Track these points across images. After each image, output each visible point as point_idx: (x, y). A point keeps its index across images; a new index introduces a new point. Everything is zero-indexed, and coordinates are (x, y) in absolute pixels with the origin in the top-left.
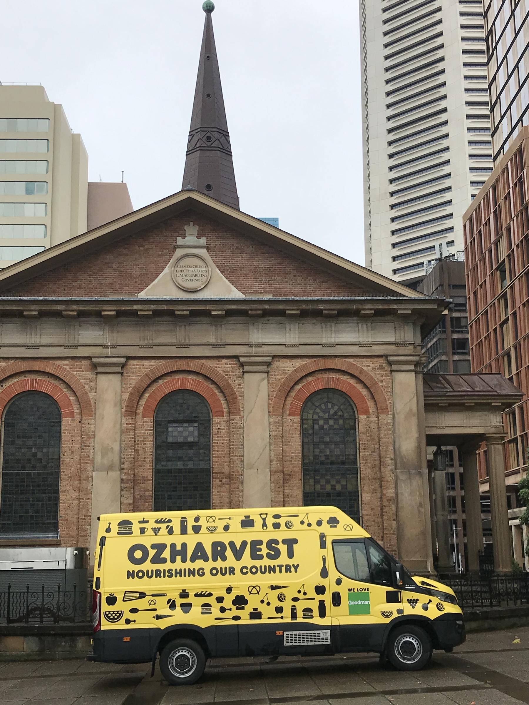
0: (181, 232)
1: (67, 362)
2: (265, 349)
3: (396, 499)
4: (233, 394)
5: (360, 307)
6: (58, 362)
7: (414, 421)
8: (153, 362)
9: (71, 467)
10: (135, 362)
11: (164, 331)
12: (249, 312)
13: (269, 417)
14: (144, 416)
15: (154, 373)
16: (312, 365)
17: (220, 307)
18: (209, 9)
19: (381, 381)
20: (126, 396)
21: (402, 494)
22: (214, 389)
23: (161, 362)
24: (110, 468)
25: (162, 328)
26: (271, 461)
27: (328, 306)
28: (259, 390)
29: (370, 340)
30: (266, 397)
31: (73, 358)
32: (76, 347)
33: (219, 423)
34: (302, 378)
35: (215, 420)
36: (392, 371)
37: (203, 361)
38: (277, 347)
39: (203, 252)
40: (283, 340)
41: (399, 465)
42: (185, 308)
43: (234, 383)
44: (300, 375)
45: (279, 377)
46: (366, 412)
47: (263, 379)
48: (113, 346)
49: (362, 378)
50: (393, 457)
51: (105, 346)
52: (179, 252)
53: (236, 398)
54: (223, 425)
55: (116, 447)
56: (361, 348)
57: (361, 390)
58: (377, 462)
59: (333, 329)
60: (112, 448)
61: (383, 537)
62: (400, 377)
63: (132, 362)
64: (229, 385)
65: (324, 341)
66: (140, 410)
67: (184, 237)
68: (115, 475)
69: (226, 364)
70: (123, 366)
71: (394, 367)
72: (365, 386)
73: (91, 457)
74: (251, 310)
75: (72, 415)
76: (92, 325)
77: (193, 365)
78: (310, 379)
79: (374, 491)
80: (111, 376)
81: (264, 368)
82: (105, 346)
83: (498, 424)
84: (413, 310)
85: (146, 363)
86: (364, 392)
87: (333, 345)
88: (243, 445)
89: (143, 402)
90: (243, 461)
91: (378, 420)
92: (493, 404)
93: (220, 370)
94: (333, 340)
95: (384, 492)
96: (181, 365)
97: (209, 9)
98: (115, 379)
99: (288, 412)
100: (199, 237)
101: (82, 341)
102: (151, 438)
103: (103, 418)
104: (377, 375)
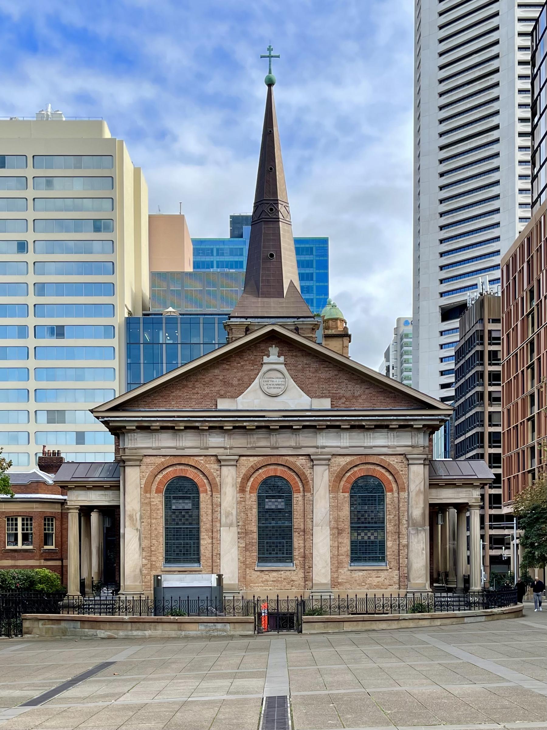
3: (407, 546)
4: (306, 478)
6: (196, 458)
8: (256, 458)
9: (207, 524)
13: (330, 494)
14: (250, 493)
15: (256, 465)
19: (402, 471)
22: (294, 475)
24: (230, 525)
26: (330, 522)
28: (323, 476)
29: (395, 444)
31: (205, 456)
32: (207, 448)
33: (297, 498)
36: (408, 464)
37: (288, 458)
40: (338, 444)
41: (411, 524)
43: (308, 472)
44: (349, 467)
45: (336, 468)
47: (326, 470)
48: (231, 448)
51: (225, 448)
53: (308, 481)
56: (389, 449)
57: (388, 476)
58: (397, 522)
59: (371, 436)
61: (399, 568)
62: (412, 468)
64: (304, 473)
65: (365, 445)
66: (248, 489)
68: (234, 530)
69: (302, 459)
77: (281, 460)
78: (356, 469)
80: (230, 467)
82: (225, 448)
85: (251, 459)
86: (390, 478)
87: (371, 447)
89: (250, 484)
93: (298, 463)
95: (401, 541)
96: (273, 460)
98: (232, 470)
99: (341, 491)
101: (211, 445)
102: (255, 506)
103: (225, 494)
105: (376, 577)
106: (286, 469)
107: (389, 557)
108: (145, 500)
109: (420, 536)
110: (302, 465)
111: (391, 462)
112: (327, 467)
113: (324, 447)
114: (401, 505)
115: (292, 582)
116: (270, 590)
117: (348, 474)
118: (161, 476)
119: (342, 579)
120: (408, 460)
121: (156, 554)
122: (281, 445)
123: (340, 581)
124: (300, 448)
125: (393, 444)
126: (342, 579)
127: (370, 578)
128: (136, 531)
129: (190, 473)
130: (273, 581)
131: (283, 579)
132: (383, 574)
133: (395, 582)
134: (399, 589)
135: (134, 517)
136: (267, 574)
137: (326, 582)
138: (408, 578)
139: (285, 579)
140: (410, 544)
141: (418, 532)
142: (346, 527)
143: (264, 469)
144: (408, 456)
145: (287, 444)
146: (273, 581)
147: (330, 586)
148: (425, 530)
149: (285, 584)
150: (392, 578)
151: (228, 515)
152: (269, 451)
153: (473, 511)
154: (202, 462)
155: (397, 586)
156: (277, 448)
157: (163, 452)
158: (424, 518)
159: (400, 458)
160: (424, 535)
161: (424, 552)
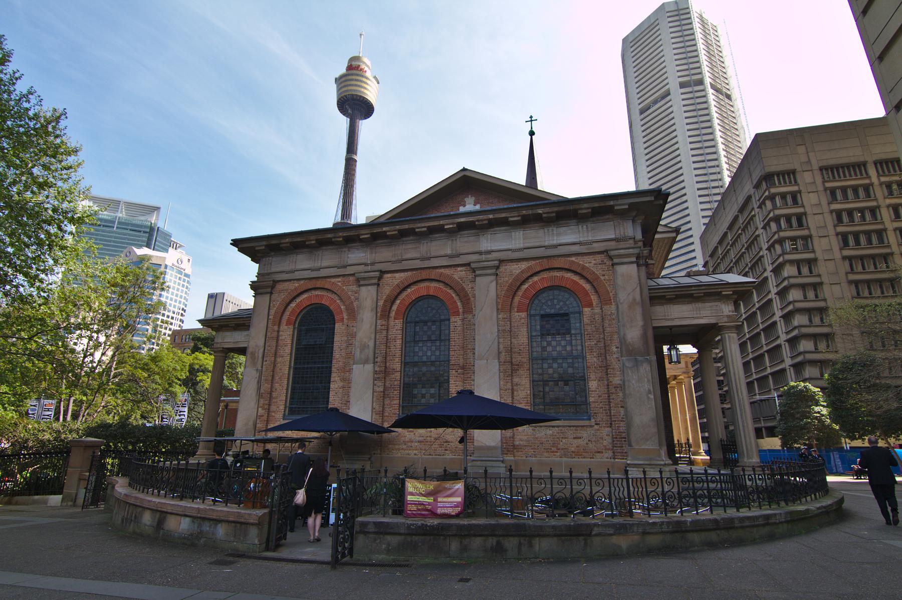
0: (463, 203)
1: (339, 279)
2: (494, 256)
3: (622, 387)
4: (466, 295)
5: (577, 207)
6: (333, 280)
8: (402, 274)
9: (339, 361)
10: (389, 275)
11: (412, 248)
12: (477, 223)
13: (498, 314)
14: (395, 319)
15: (403, 283)
16: (535, 265)
17: (450, 221)
18: (532, 133)
19: (603, 275)
20: (381, 303)
21: (629, 381)
22: (452, 293)
23: (409, 273)
24: (366, 362)
25: (410, 246)
26: (499, 353)
27: (547, 210)
28: (488, 291)
29: (590, 238)
30: (495, 297)
31: (343, 276)
32: (345, 267)
33: (456, 322)
34: (528, 278)
36: (613, 265)
37: (442, 270)
38: (504, 252)
40: (510, 247)
41: (624, 352)
42: (423, 225)
43: (468, 287)
44: (525, 276)
45: (507, 279)
46: (590, 305)
47: (492, 282)
48: (373, 264)
49: (584, 274)
50: (618, 345)
51: (366, 264)
53: (469, 299)
54: (459, 323)
55: (371, 344)
56: (582, 247)
57: (584, 285)
58: (603, 351)
59: (555, 232)
60: (368, 345)
61: (611, 424)
62: (621, 269)
63: (386, 276)
64: (463, 289)
65: (546, 244)
66: (393, 314)
67: (464, 206)
68: (369, 367)
69: (461, 271)
70: (380, 278)
71: (616, 261)
72: (588, 281)
73: (353, 353)
74: (478, 221)
75: (342, 320)
76: (358, 249)
77: (433, 274)
78: (536, 279)
79: (600, 379)
80: (369, 287)
81: (493, 271)
82: (366, 264)
83: (731, 313)
84: (630, 205)
85: (397, 275)
86: (587, 287)
87: (555, 246)
88: (474, 339)
89: (395, 307)
90: (474, 354)
91: (602, 312)
92: (723, 293)
93: (456, 277)
94: (555, 242)
95: (611, 379)
96: (424, 275)
97: (532, 133)
98: (373, 289)
99: (516, 310)
100: (475, 205)
101: (350, 262)
102: (400, 337)
103: (362, 321)
104: (598, 272)
105: (575, 438)
106: (441, 286)
107: (593, 405)
108: (272, 333)
109: (642, 370)
110: (461, 279)
111: (587, 265)
112: (493, 277)
113: (489, 252)
114: (606, 325)
115: (445, 444)
116: (415, 454)
117: (525, 286)
118: (294, 305)
119: (521, 440)
120: (611, 258)
121: (276, 402)
122: (433, 254)
123: (517, 443)
124: (459, 255)
125: (586, 239)
126: (521, 440)
127: (564, 441)
128: (255, 372)
129: (326, 299)
130: (419, 442)
131: (433, 439)
132: (585, 434)
133: (605, 446)
134: (615, 459)
135: (256, 355)
136: (411, 431)
137: (493, 444)
138: (627, 440)
139: (436, 439)
140: (626, 383)
141: (637, 364)
142: (524, 360)
143: (413, 288)
144: (612, 253)
145: (442, 253)
146: (419, 442)
147: (499, 451)
148: (650, 362)
149: (437, 446)
150: (601, 441)
151: (364, 347)
152: (418, 264)
153: (727, 335)
154: (339, 284)
155: (610, 454)
156: (429, 259)
157: (297, 275)
158: (646, 343)
159: (599, 258)
160: (648, 368)
161: (652, 397)
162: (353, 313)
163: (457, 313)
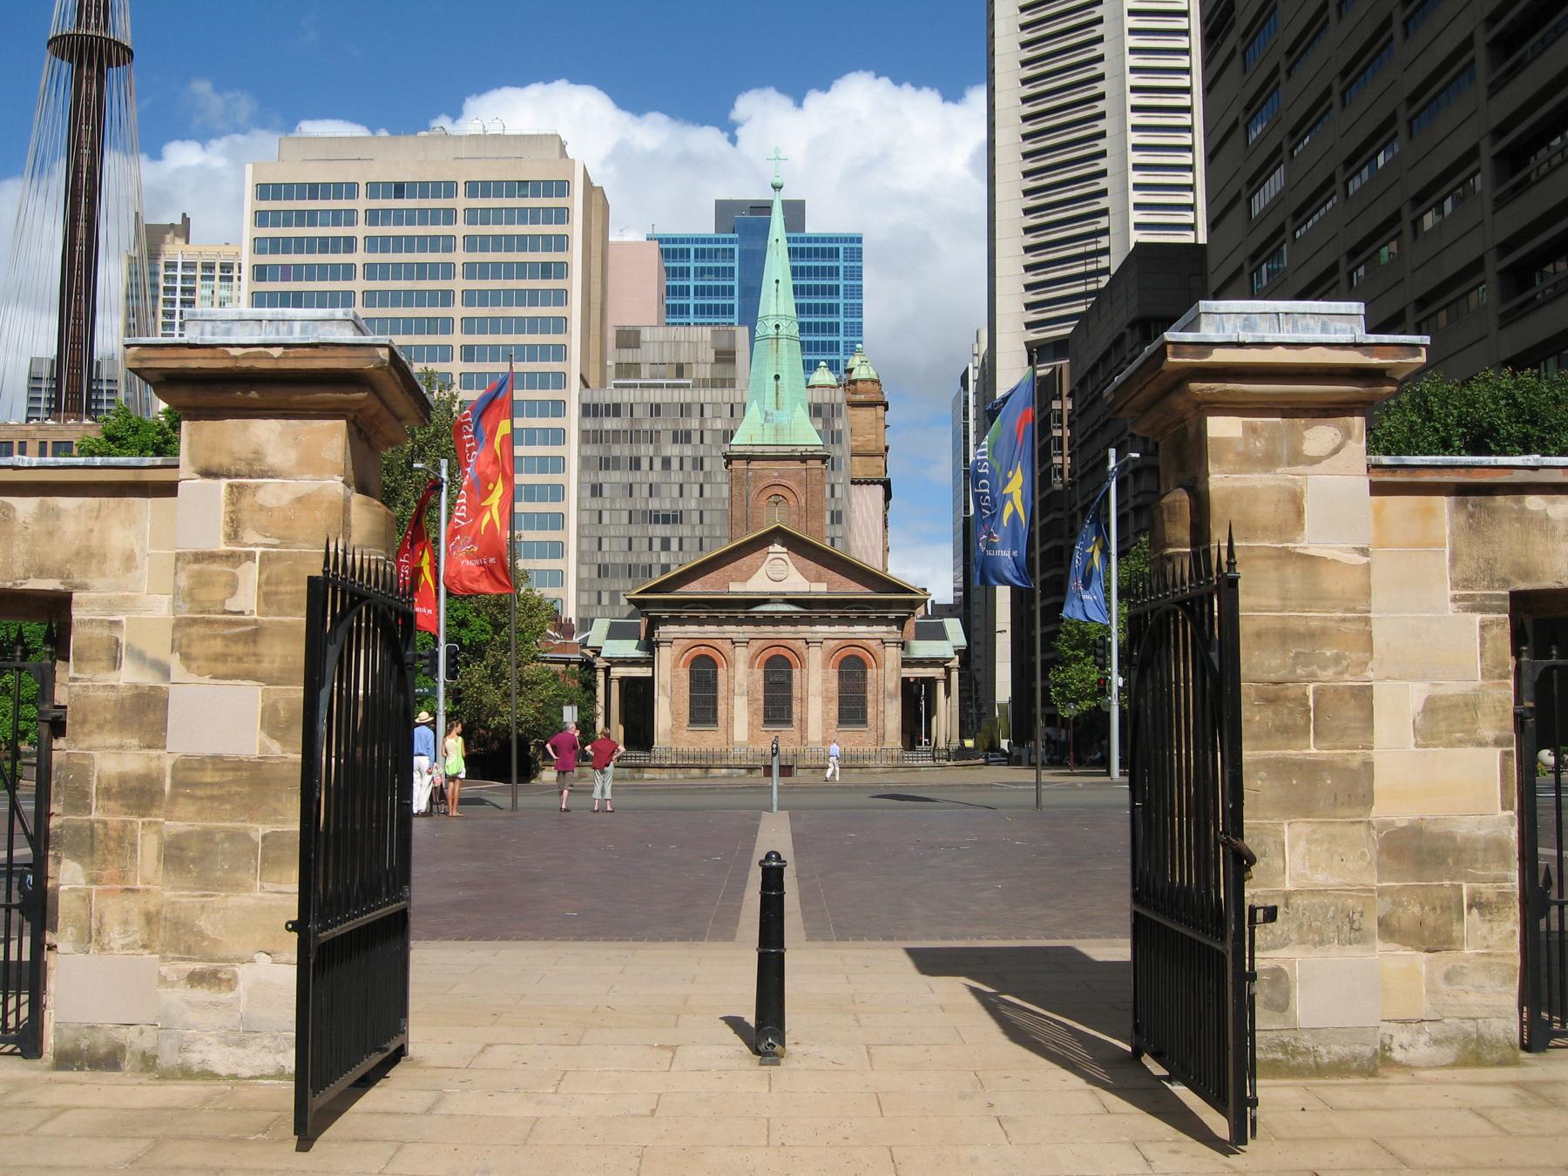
7: (895, 672)
16: (844, 643)
24: (742, 695)
35: (794, 670)
39: (785, 557)
46: (871, 667)
52: (771, 556)
55: (745, 684)
68: (745, 698)
77: (783, 643)
96: (776, 642)
132: (864, 735)
137: (817, 739)
151: (741, 685)
162: (730, 664)
163: (797, 667)
